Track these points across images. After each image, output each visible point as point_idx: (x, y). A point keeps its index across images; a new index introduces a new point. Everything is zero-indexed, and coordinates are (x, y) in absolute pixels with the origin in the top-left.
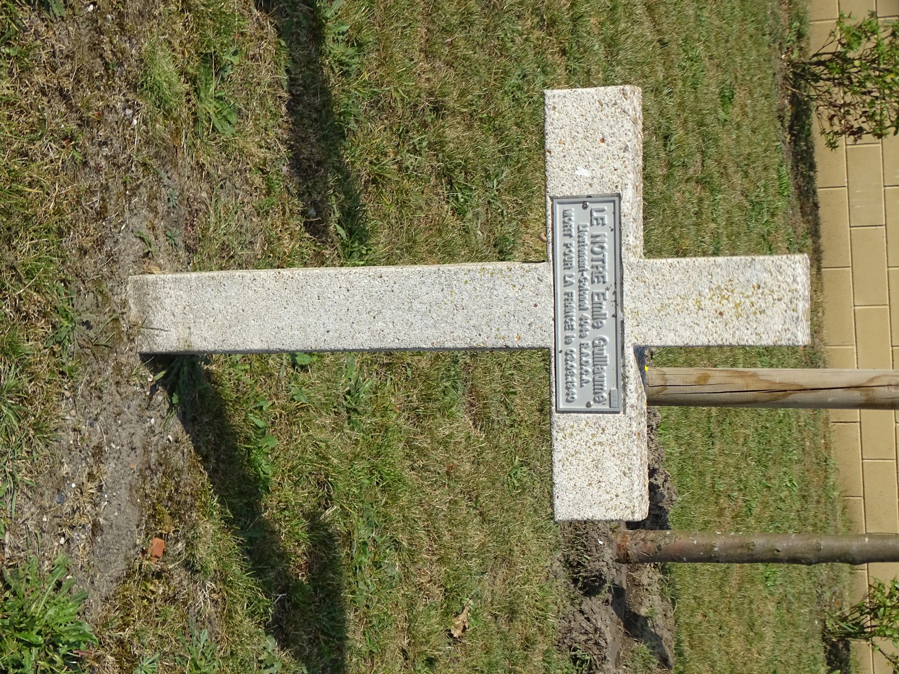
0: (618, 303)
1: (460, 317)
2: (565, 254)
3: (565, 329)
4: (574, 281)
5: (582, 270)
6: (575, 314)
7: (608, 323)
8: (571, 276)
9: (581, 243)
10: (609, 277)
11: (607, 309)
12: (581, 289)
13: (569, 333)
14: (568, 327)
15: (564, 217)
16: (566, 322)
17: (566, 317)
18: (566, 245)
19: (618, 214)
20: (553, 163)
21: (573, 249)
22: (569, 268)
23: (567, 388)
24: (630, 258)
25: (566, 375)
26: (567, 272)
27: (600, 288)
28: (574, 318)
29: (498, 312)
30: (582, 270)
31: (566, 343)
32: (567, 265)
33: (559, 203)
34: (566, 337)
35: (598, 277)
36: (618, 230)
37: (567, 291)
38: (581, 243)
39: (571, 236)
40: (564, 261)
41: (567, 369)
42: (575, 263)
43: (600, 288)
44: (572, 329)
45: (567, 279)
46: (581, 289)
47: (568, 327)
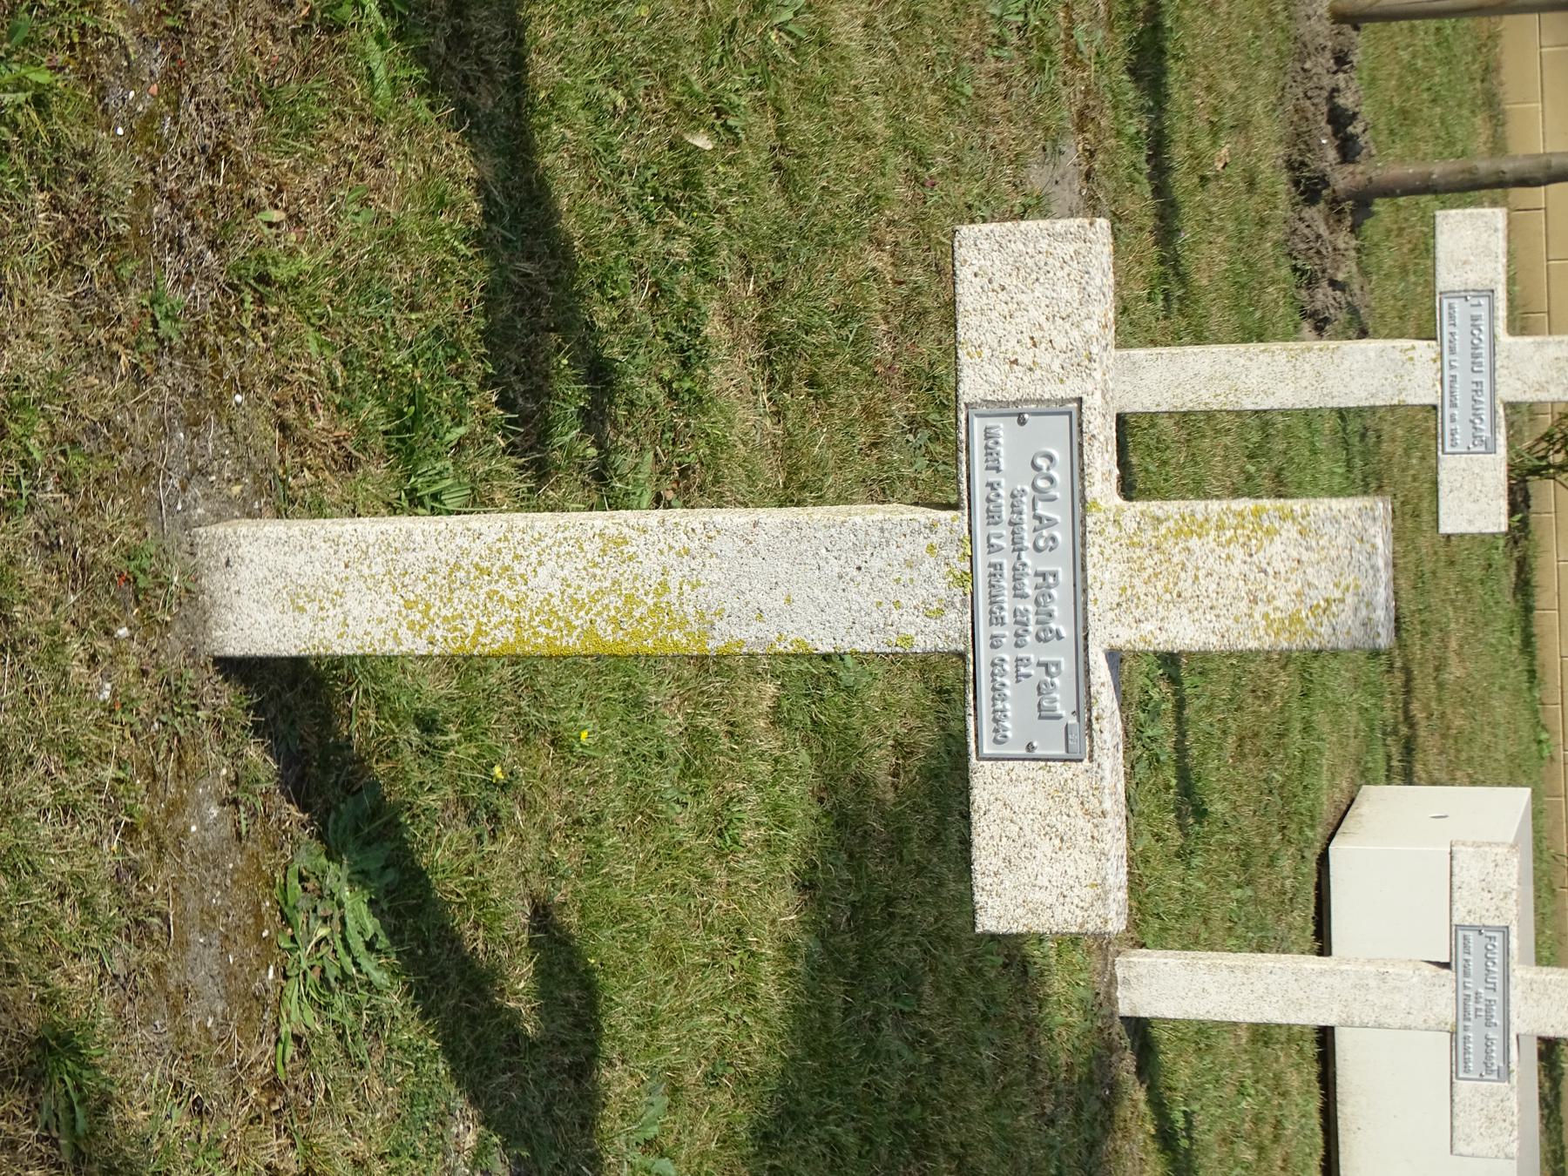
3: (991, 624)
8: (999, 536)
13: (997, 630)
16: (991, 612)
17: (992, 603)
18: (990, 485)
23: (996, 721)
25: (994, 699)
31: (992, 646)
34: (993, 637)
41: (994, 689)
42: (1006, 514)
44: (1003, 624)
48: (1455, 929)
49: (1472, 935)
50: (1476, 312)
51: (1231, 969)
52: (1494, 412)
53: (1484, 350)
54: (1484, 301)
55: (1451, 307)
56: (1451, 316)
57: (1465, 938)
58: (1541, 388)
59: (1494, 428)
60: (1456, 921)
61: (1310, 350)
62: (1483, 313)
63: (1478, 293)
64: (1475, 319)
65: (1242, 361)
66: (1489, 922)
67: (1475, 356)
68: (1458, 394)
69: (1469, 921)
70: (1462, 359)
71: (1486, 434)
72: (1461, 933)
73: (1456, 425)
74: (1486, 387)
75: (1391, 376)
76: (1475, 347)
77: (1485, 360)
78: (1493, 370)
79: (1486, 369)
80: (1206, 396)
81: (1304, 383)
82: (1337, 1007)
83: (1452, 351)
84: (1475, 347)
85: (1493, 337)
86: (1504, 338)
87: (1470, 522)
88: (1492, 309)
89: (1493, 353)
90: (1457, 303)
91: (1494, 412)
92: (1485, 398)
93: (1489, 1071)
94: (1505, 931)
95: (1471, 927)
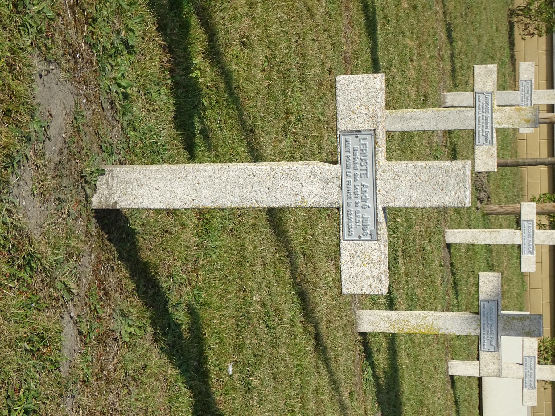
0: (531, 97)
1: (503, 100)
5: (525, 92)
6: (524, 99)
7: (529, 101)
8: (350, 172)
9: (525, 88)
10: (530, 93)
11: (529, 98)
12: (525, 95)
14: (522, 101)
15: (346, 142)
18: (347, 156)
19: (531, 83)
20: (520, 74)
24: (533, 90)
26: (348, 170)
27: (528, 95)
28: (352, 193)
29: (510, 99)
30: (525, 92)
32: (522, 91)
35: (528, 93)
36: (531, 85)
37: (348, 180)
38: (525, 88)
39: (349, 152)
40: (346, 164)
42: (352, 165)
43: (528, 95)
45: (348, 174)
46: (525, 95)
47: (522, 101)
50: (530, 225)
52: (533, 246)
53: (531, 233)
54: (531, 223)
55: (524, 224)
56: (524, 226)
58: (544, 242)
59: (533, 250)
61: (493, 231)
62: (531, 225)
63: (530, 221)
65: (478, 233)
67: (529, 234)
68: (526, 242)
70: (526, 235)
71: (532, 251)
73: (525, 249)
74: (532, 241)
76: (529, 233)
77: (531, 235)
78: (533, 237)
79: (532, 237)
80: (470, 241)
81: (492, 239)
83: (524, 233)
84: (529, 233)
85: (533, 231)
87: (528, 270)
88: (533, 225)
89: (533, 234)
90: (526, 223)
91: (533, 246)
92: (531, 243)
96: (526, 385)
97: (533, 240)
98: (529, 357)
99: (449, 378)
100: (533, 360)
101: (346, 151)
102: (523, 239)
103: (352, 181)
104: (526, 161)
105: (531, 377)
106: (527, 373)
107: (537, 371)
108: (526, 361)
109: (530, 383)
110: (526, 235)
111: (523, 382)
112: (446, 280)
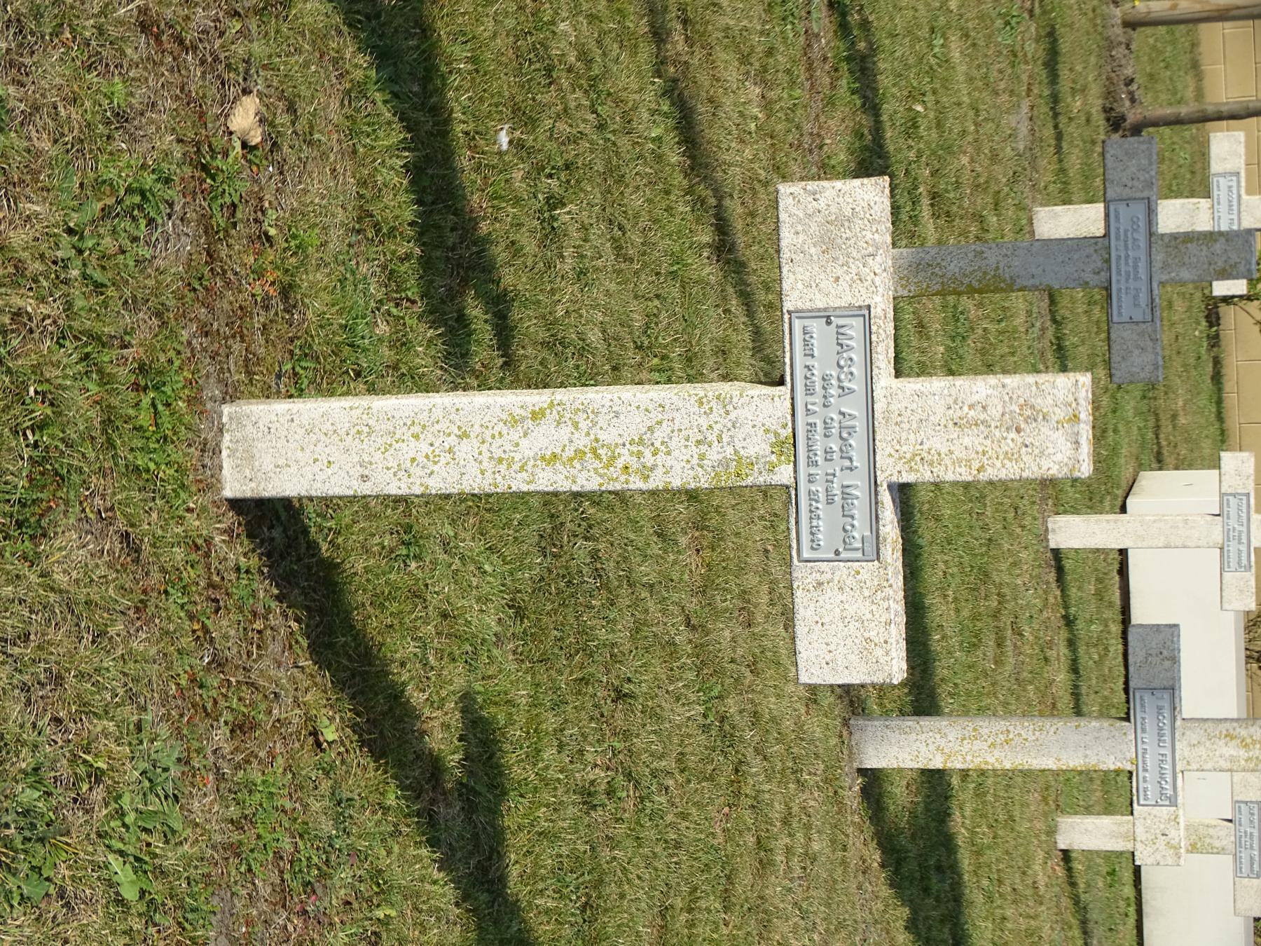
2: (806, 378)
3: (808, 466)
4: (817, 409)
8: (814, 404)
13: (813, 470)
15: (805, 334)
16: (809, 457)
17: (809, 451)
18: (807, 367)
21: (815, 372)
22: (812, 394)
23: (812, 534)
25: (811, 518)
26: (810, 399)
28: (818, 452)
31: (809, 481)
33: (798, 318)
34: (810, 475)
37: (810, 421)
39: (813, 356)
40: (806, 385)
41: (811, 511)
42: (818, 388)
44: (817, 465)
45: (809, 407)
48: (1222, 495)
49: (1231, 498)
50: (1230, 184)
51: (1108, 521)
53: (1235, 203)
54: (1234, 178)
55: (1218, 181)
56: (1218, 186)
57: (1228, 500)
60: (1223, 491)
62: (1234, 184)
63: (1231, 174)
64: (1230, 187)
66: (1239, 491)
67: (1230, 206)
69: (1230, 491)
70: (1223, 207)
72: (1225, 498)
75: (1188, 217)
77: (1235, 208)
79: (1235, 212)
82: (1162, 538)
83: (1219, 203)
84: (1230, 201)
85: (1239, 196)
86: (1244, 197)
87: (1228, 289)
88: (1239, 182)
93: (1241, 567)
94: (1248, 495)
95: (1230, 494)
96: (1229, 562)
97: (1239, 219)
98: (1234, 495)
99: (1049, 555)
100: (1244, 502)
101: (805, 355)
102: (1216, 218)
103: (818, 425)
104: (1224, 109)
105: (1240, 543)
106: (1231, 533)
107: (1253, 527)
108: (1228, 504)
109: (1240, 557)
110: (1223, 207)
111: (1222, 556)
112: (1038, 324)
